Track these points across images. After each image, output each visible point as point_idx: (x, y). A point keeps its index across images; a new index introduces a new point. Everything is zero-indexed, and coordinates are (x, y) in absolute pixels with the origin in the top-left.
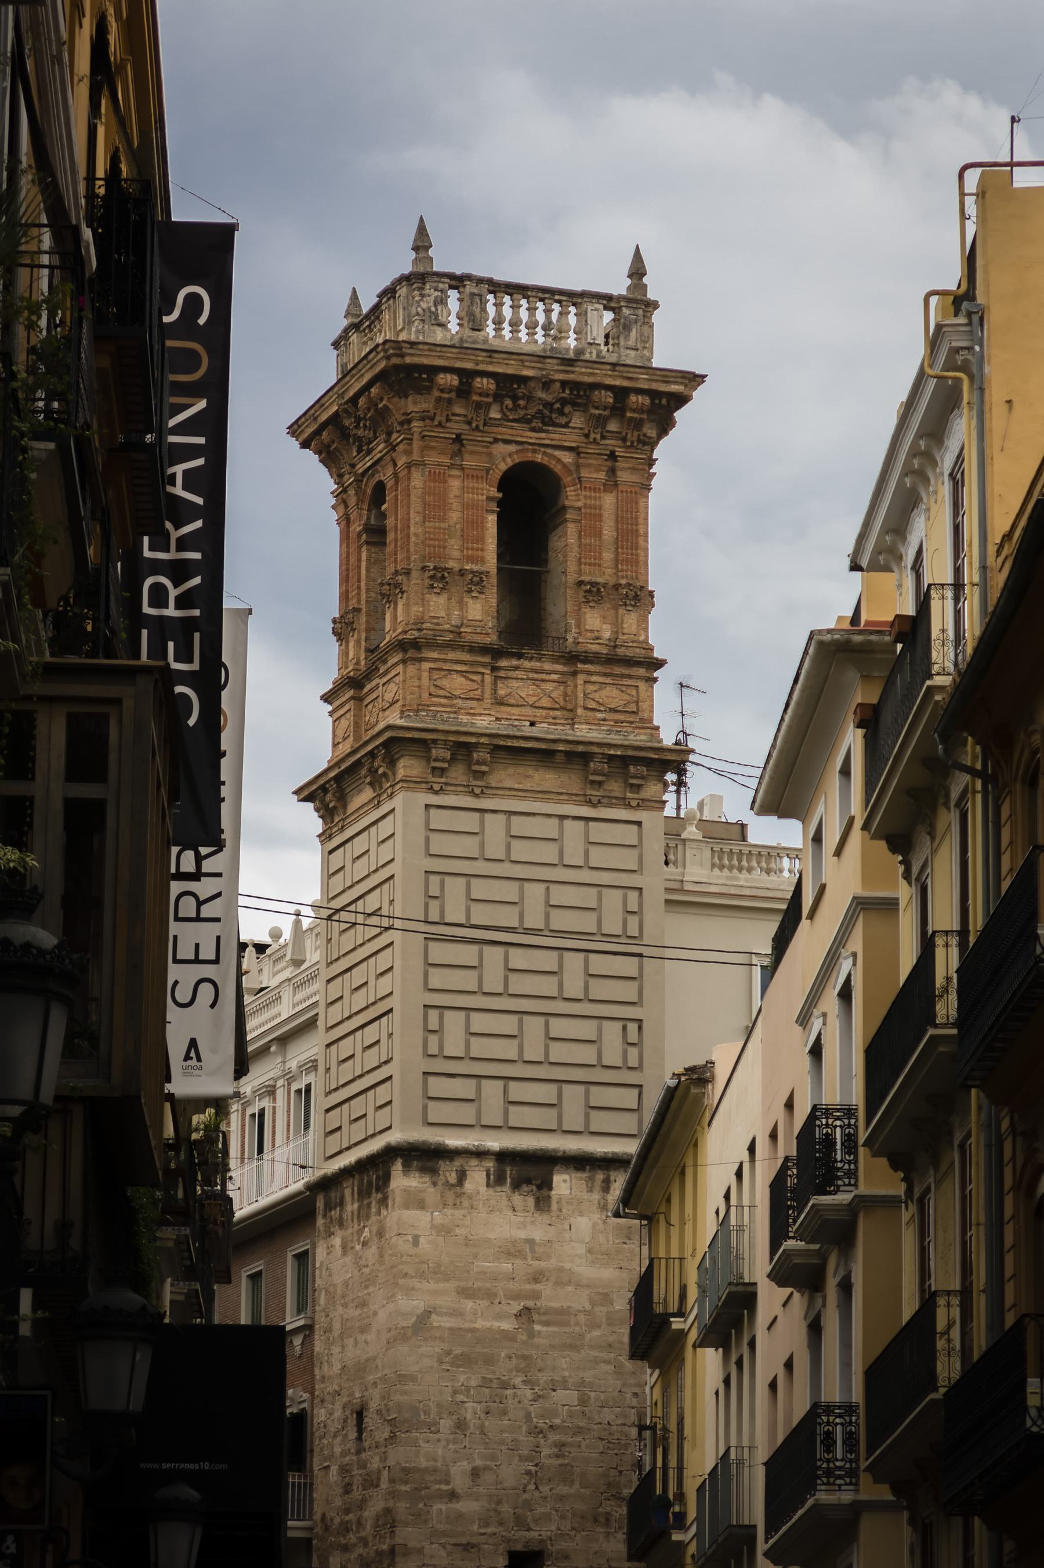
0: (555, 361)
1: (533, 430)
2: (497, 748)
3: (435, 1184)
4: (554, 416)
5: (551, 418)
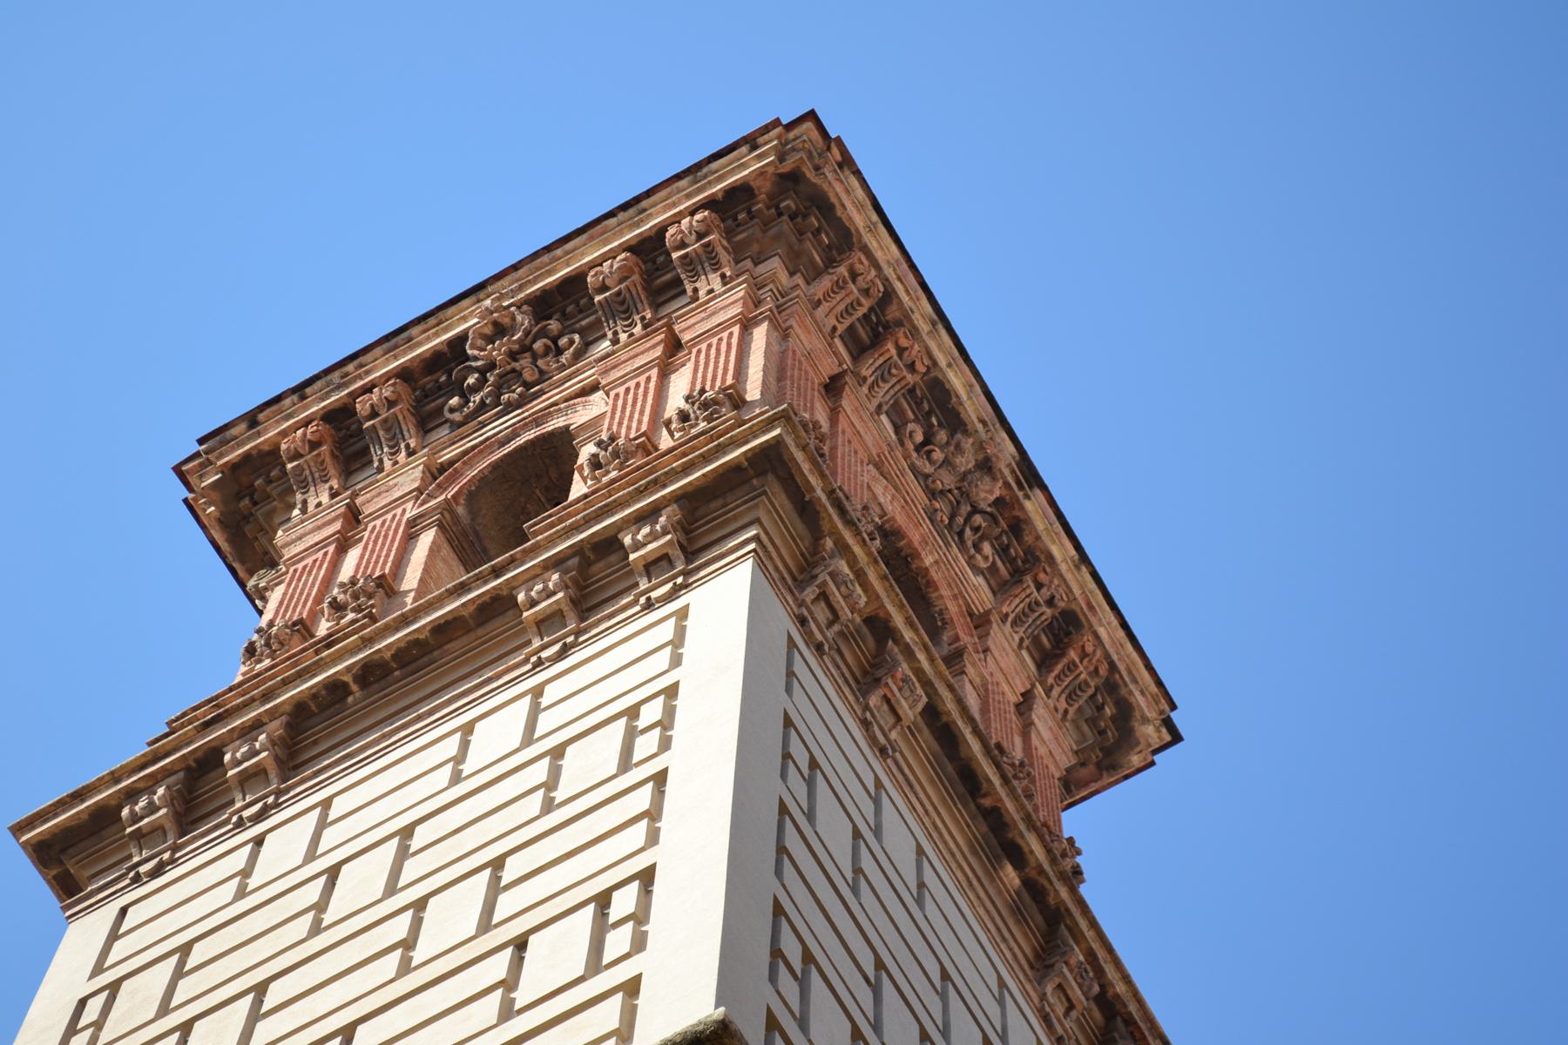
0: (1012, 449)
1: (931, 515)
2: (932, 713)
4: (968, 532)
5: (961, 534)
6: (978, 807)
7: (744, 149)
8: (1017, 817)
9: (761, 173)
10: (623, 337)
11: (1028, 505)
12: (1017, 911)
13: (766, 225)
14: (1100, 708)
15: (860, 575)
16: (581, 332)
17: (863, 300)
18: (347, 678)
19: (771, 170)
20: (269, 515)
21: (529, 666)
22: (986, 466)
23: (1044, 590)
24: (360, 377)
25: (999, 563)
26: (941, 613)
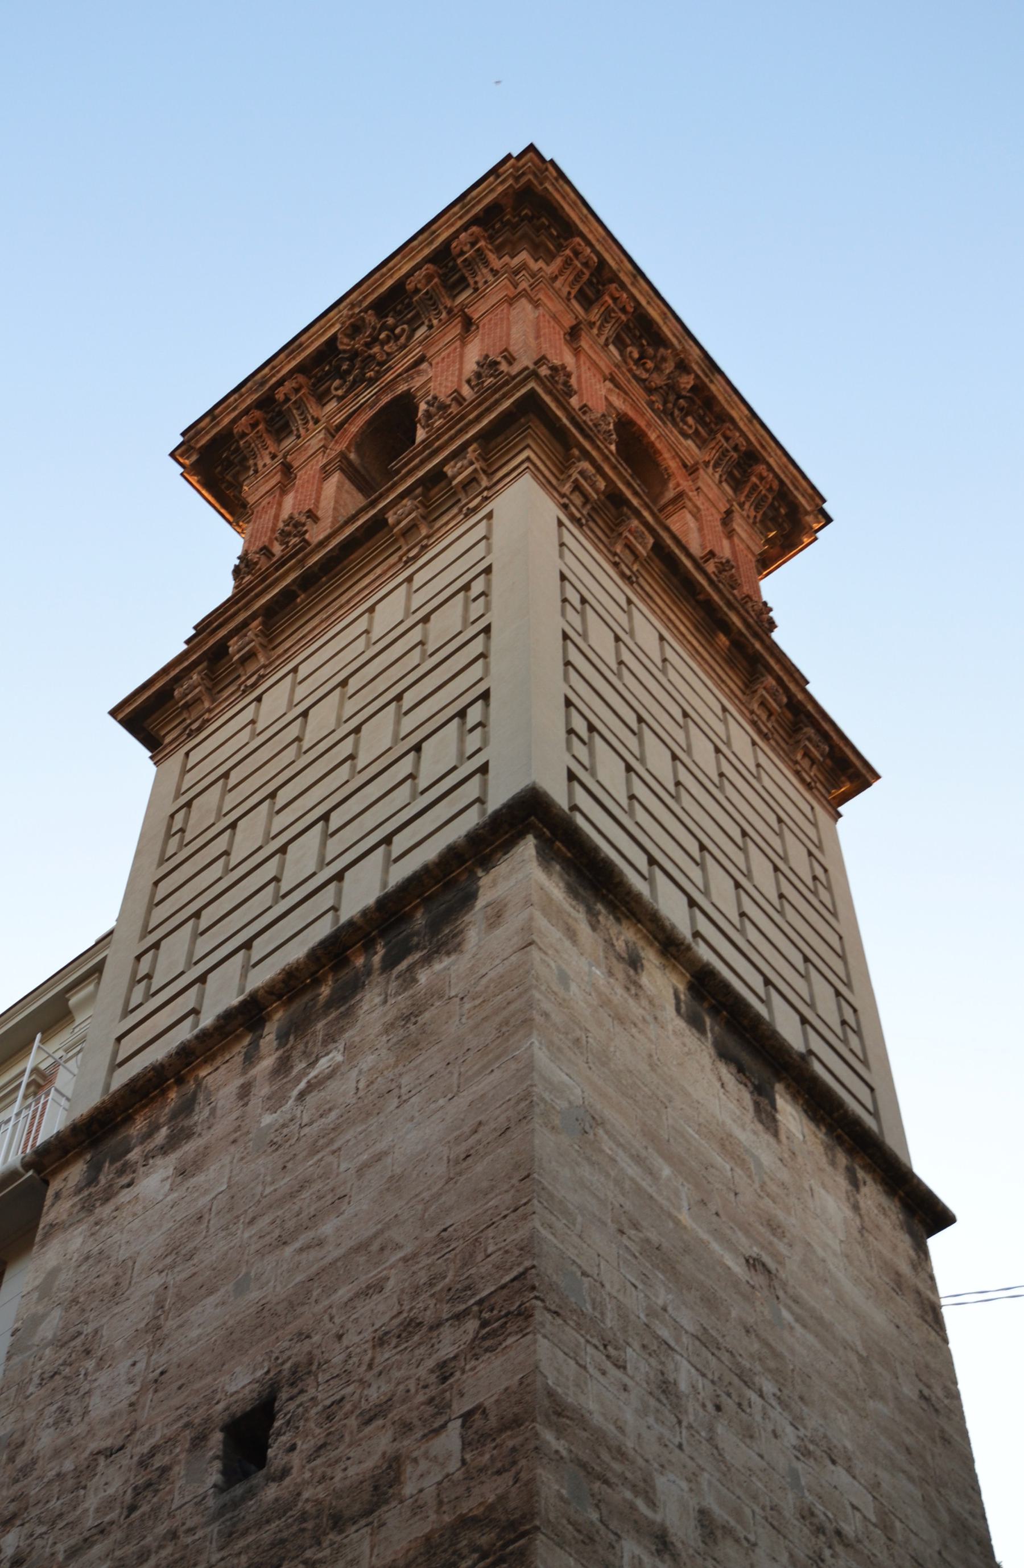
0: (698, 351)
1: (651, 404)
3: (594, 928)
4: (676, 412)
6: (697, 601)
7: (491, 179)
8: (721, 603)
9: (504, 193)
10: (435, 322)
11: (713, 387)
12: (730, 662)
13: (514, 227)
14: (777, 510)
15: (599, 470)
16: (408, 322)
17: (585, 270)
18: (294, 588)
19: (511, 191)
20: (236, 476)
21: (401, 565)
22: (683, 367)
23: (731, 441)
24: (273, 375)
25: (700, 429)
26: (666, 469)
